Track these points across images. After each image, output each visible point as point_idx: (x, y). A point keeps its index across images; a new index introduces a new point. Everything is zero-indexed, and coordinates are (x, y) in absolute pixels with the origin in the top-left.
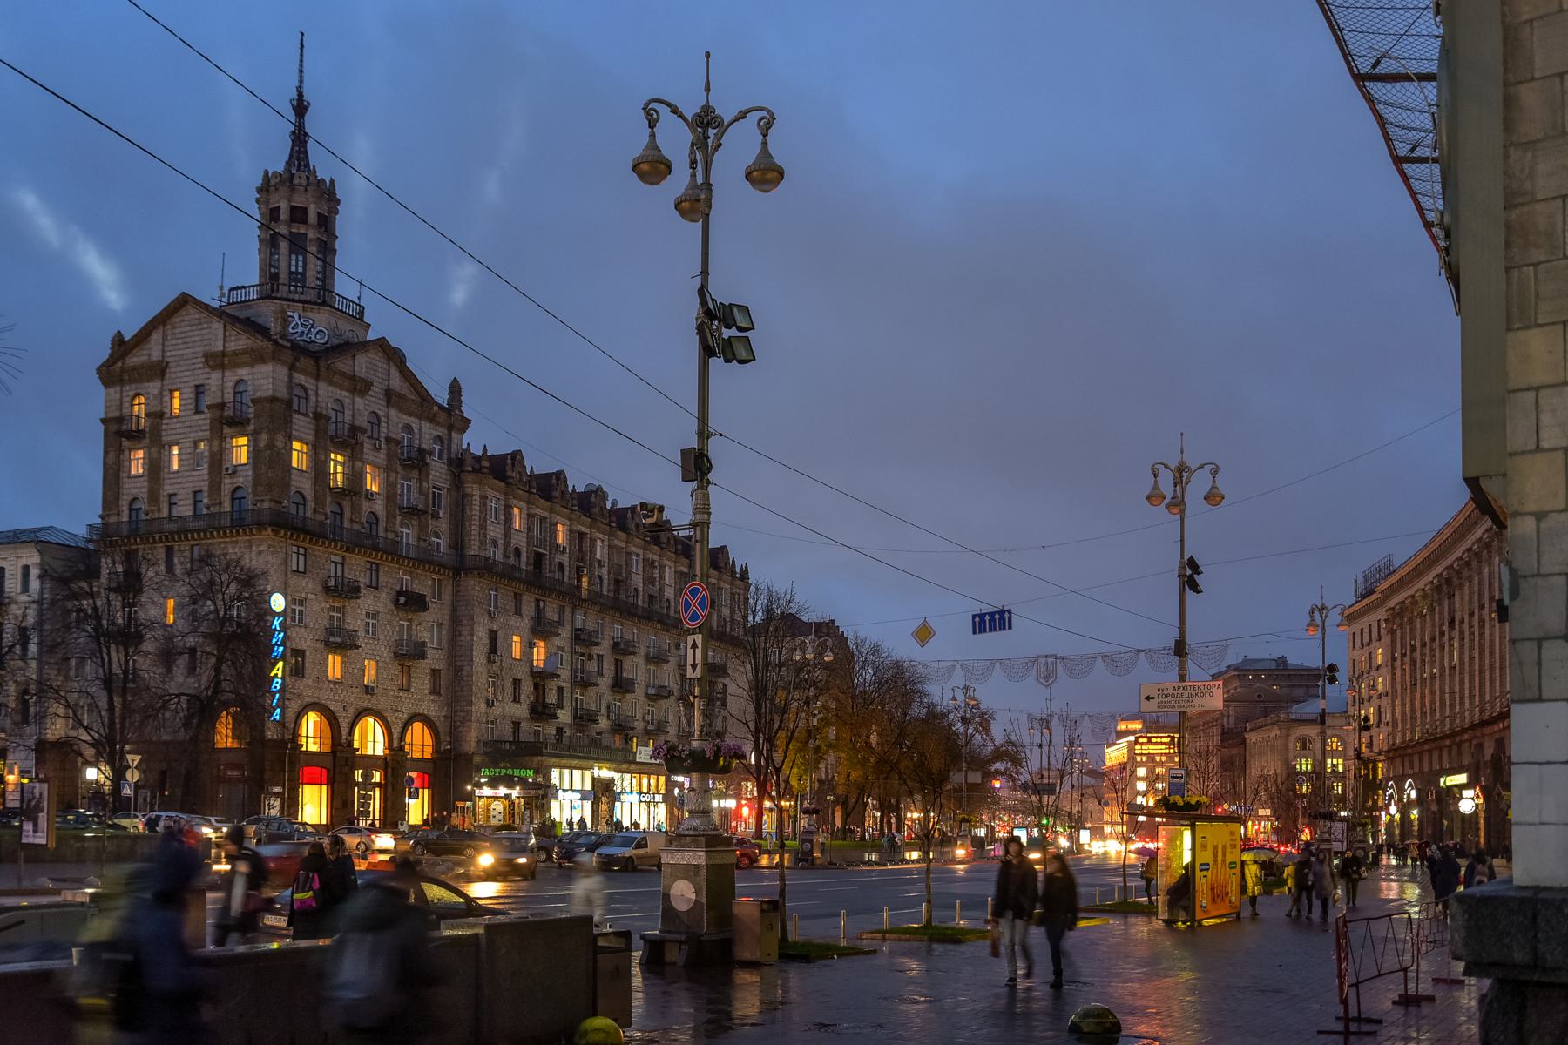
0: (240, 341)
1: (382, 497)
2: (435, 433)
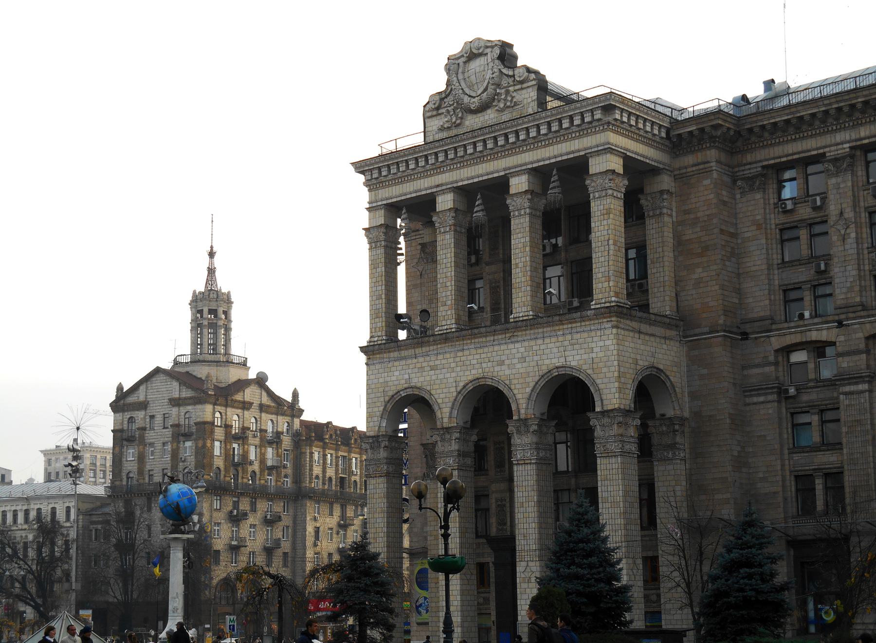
0: (187, 393)
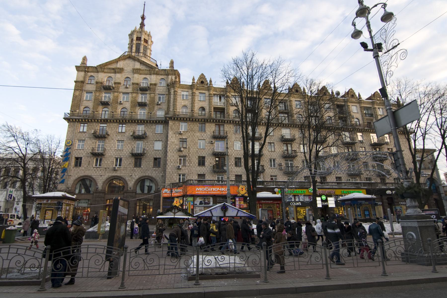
1: (129, 102)
2: (160, 78)
